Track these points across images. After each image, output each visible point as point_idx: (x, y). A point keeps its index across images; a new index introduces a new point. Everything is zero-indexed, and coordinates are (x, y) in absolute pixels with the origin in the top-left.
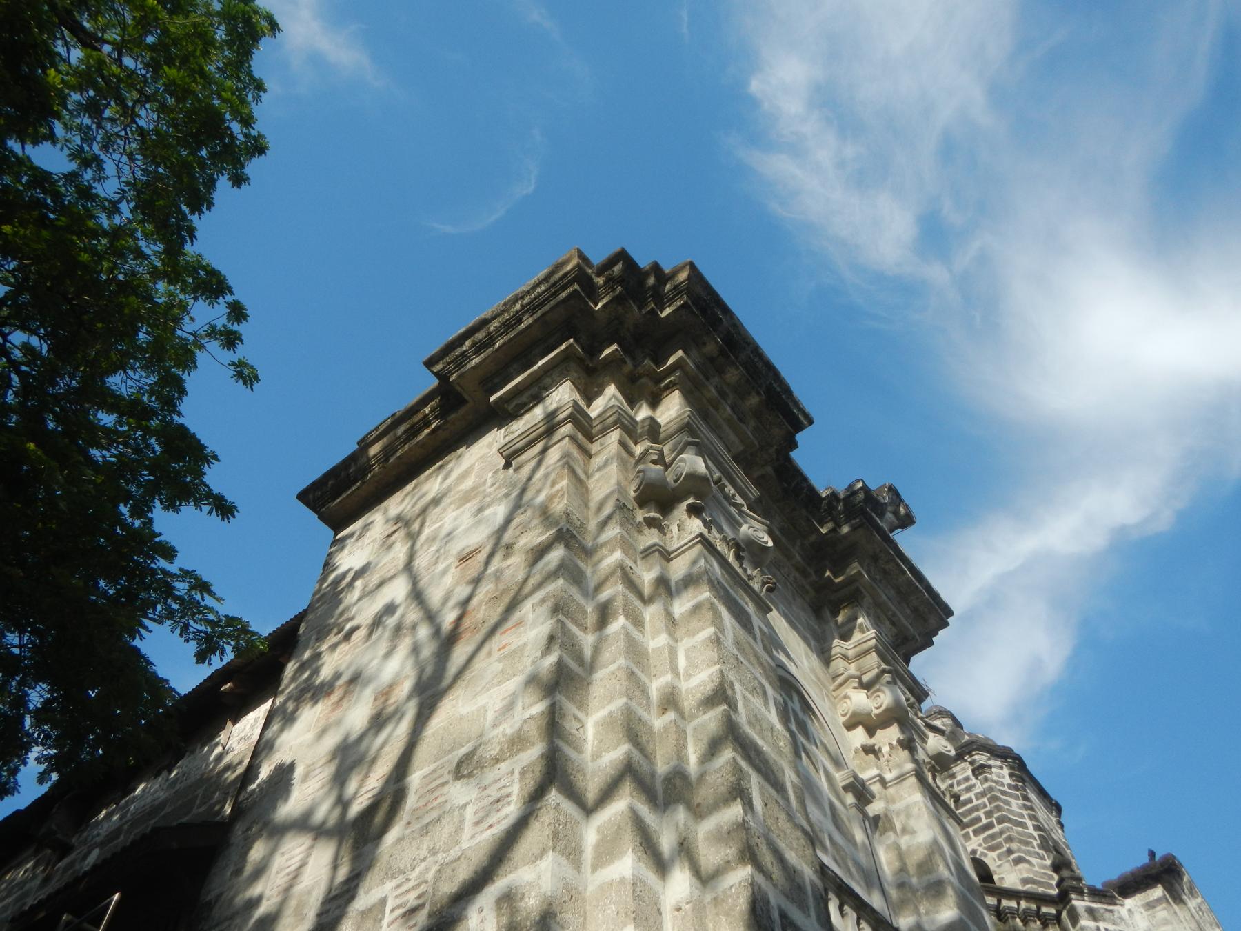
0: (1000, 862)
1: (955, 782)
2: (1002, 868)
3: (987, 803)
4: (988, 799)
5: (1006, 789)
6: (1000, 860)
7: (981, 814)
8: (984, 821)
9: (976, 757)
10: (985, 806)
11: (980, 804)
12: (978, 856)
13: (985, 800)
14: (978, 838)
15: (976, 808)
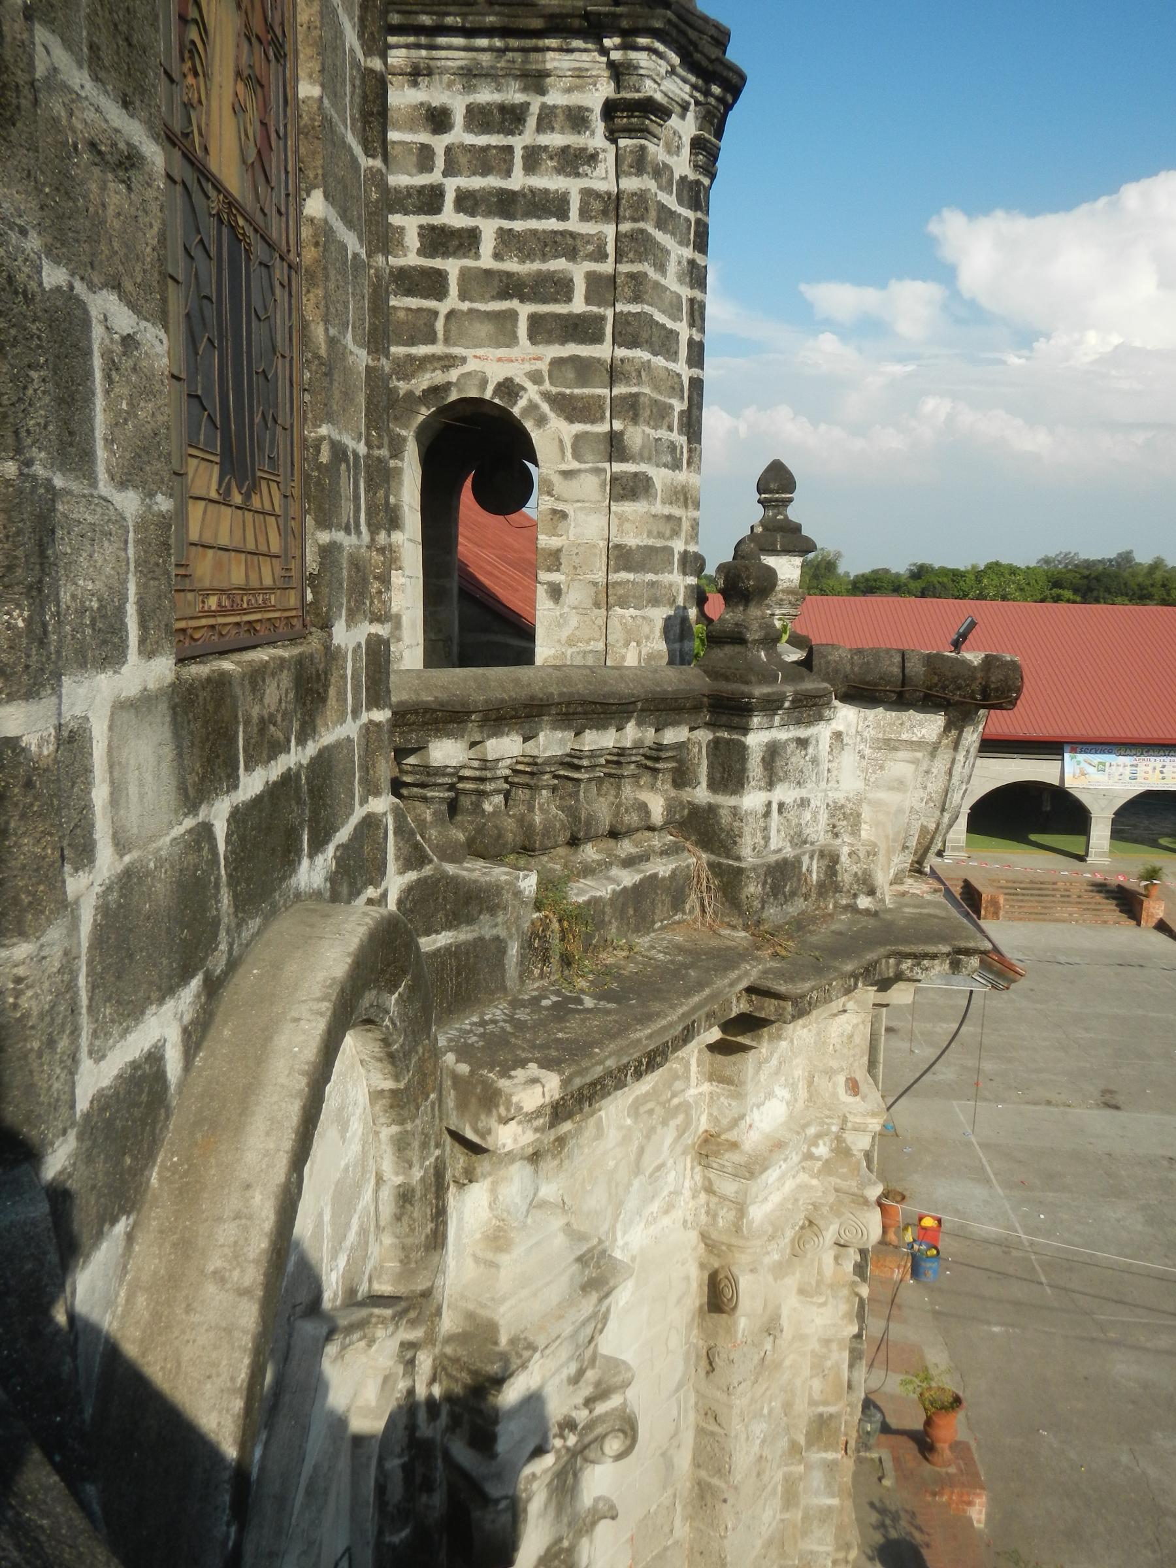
0: (575, 465)
1: (535, 109)
2: (574, 483)
3: (610, 249)
4: (618, 237)
5: (670, 201)
6: (577, 456)
7: (579, 272)
8: (578, 305)
9: (641, 58)
10: (602, 256)
11: (587, 239)
12: (516, 411)
13: (609, 231)
14: (540, 350)
15: (567, 245)
